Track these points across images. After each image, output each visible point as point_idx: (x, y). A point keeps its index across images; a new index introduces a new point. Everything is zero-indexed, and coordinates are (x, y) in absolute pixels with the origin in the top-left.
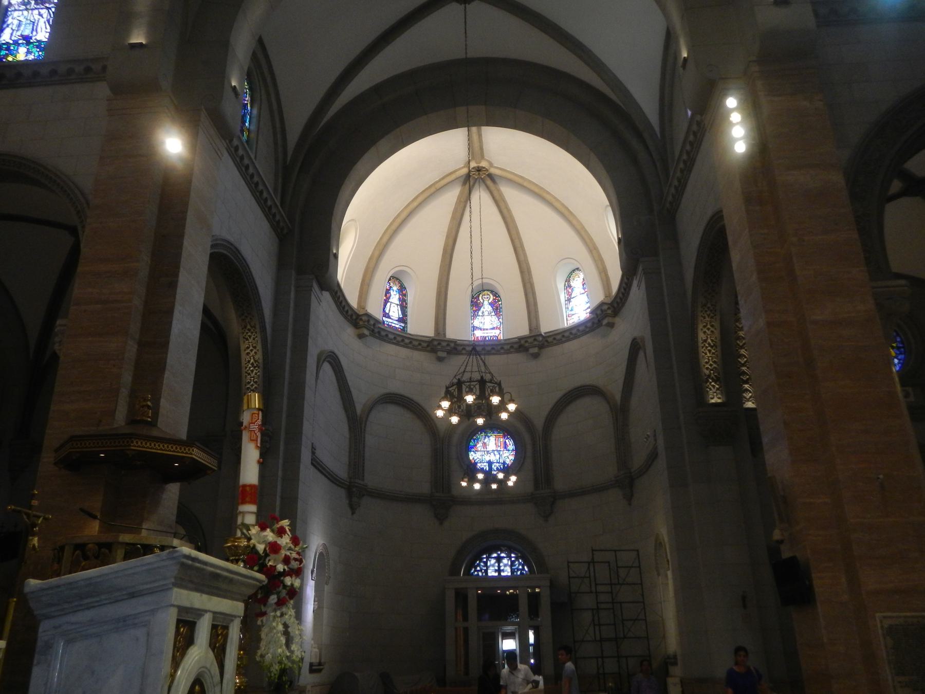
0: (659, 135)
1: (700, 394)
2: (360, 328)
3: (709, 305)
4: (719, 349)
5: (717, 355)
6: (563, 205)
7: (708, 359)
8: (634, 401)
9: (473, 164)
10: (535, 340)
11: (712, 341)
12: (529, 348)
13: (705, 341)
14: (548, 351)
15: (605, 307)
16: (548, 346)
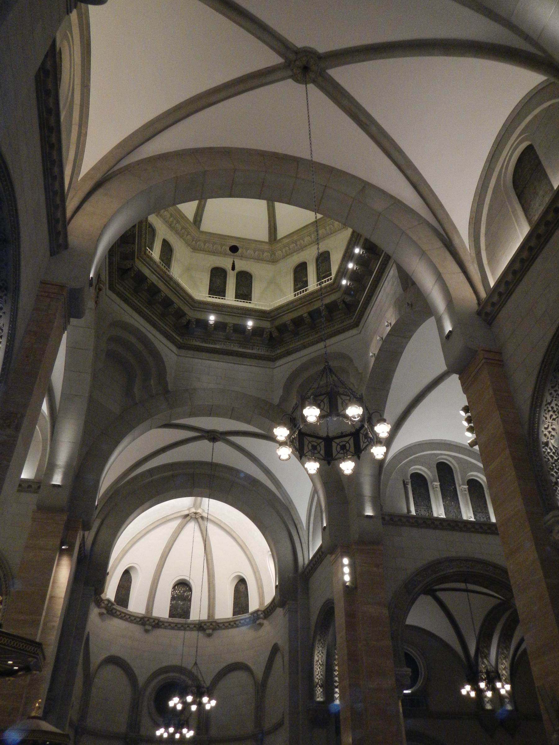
0: (305, 529)
1: (312, 695)
2: (100, 608)
3: (322, 640)
4: (324, 667)
5: (323, 671)
6: (242, 541)
7: (318, 672)
8: (271, 681)
9: (193, 510)
10: (211, 624)
11: (321, 661)
12: (206, 629)
13: (318, 661)
14: (217, 633)
15: (260, 613)
16: (218, 629)
